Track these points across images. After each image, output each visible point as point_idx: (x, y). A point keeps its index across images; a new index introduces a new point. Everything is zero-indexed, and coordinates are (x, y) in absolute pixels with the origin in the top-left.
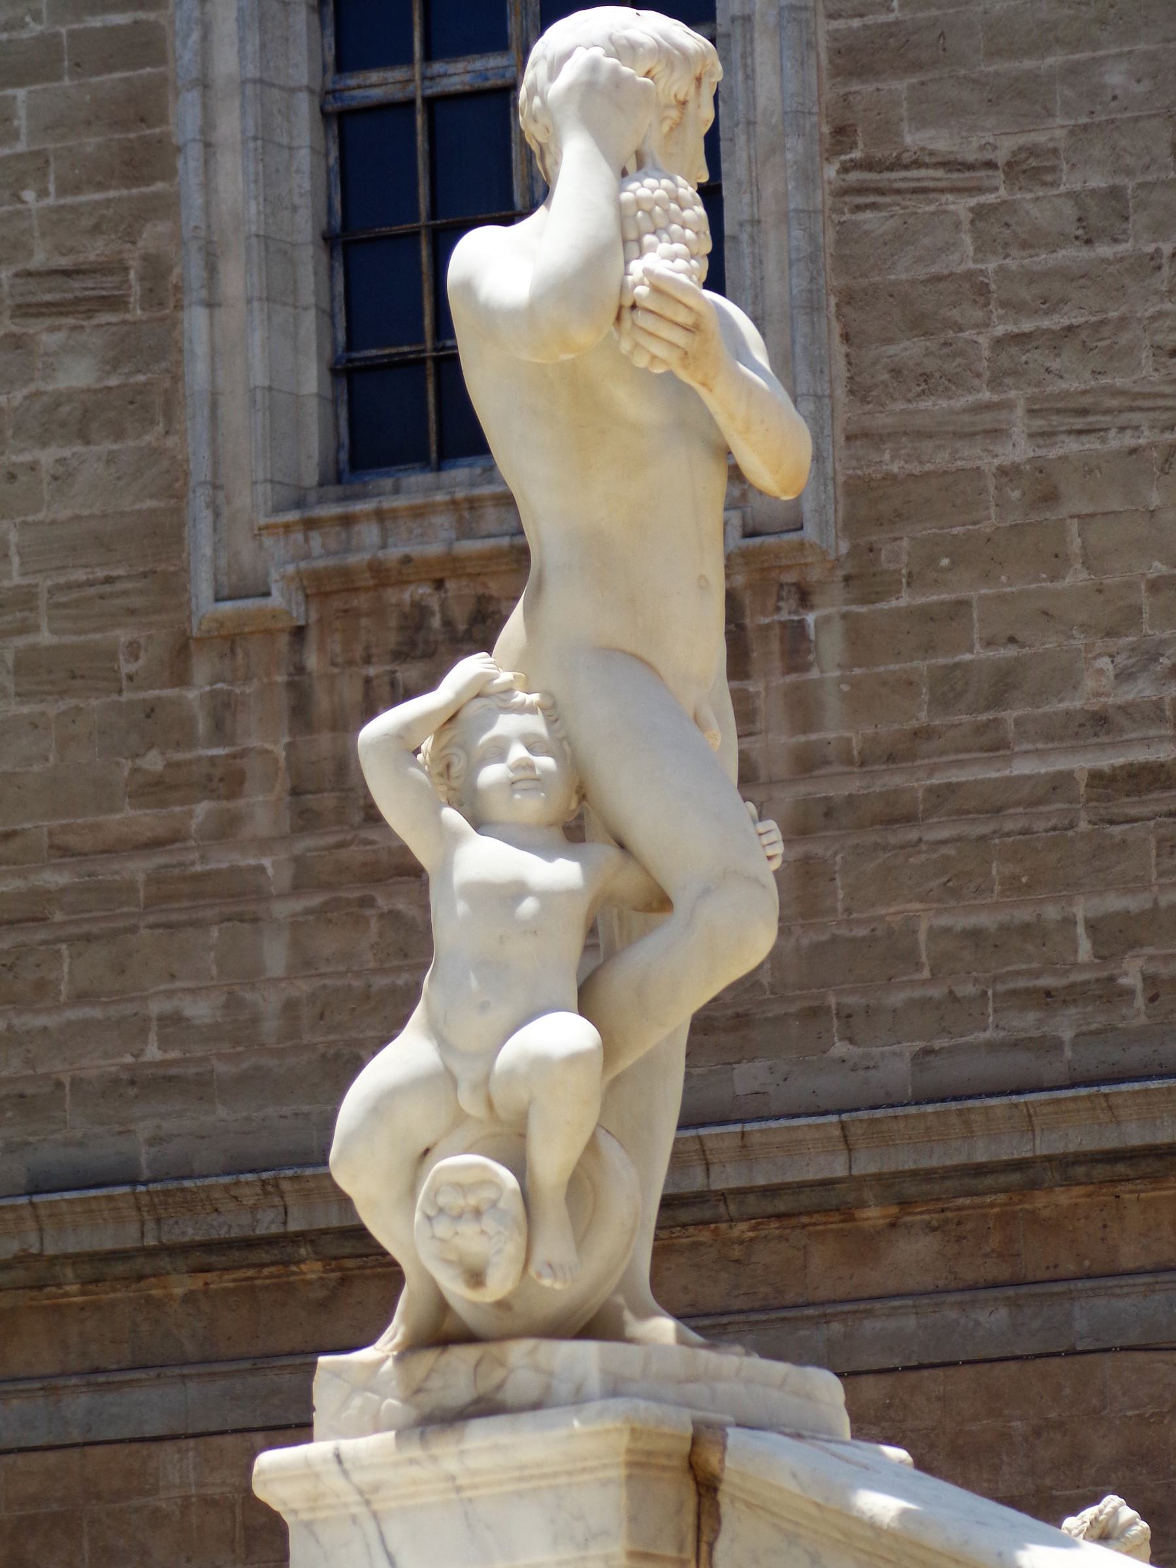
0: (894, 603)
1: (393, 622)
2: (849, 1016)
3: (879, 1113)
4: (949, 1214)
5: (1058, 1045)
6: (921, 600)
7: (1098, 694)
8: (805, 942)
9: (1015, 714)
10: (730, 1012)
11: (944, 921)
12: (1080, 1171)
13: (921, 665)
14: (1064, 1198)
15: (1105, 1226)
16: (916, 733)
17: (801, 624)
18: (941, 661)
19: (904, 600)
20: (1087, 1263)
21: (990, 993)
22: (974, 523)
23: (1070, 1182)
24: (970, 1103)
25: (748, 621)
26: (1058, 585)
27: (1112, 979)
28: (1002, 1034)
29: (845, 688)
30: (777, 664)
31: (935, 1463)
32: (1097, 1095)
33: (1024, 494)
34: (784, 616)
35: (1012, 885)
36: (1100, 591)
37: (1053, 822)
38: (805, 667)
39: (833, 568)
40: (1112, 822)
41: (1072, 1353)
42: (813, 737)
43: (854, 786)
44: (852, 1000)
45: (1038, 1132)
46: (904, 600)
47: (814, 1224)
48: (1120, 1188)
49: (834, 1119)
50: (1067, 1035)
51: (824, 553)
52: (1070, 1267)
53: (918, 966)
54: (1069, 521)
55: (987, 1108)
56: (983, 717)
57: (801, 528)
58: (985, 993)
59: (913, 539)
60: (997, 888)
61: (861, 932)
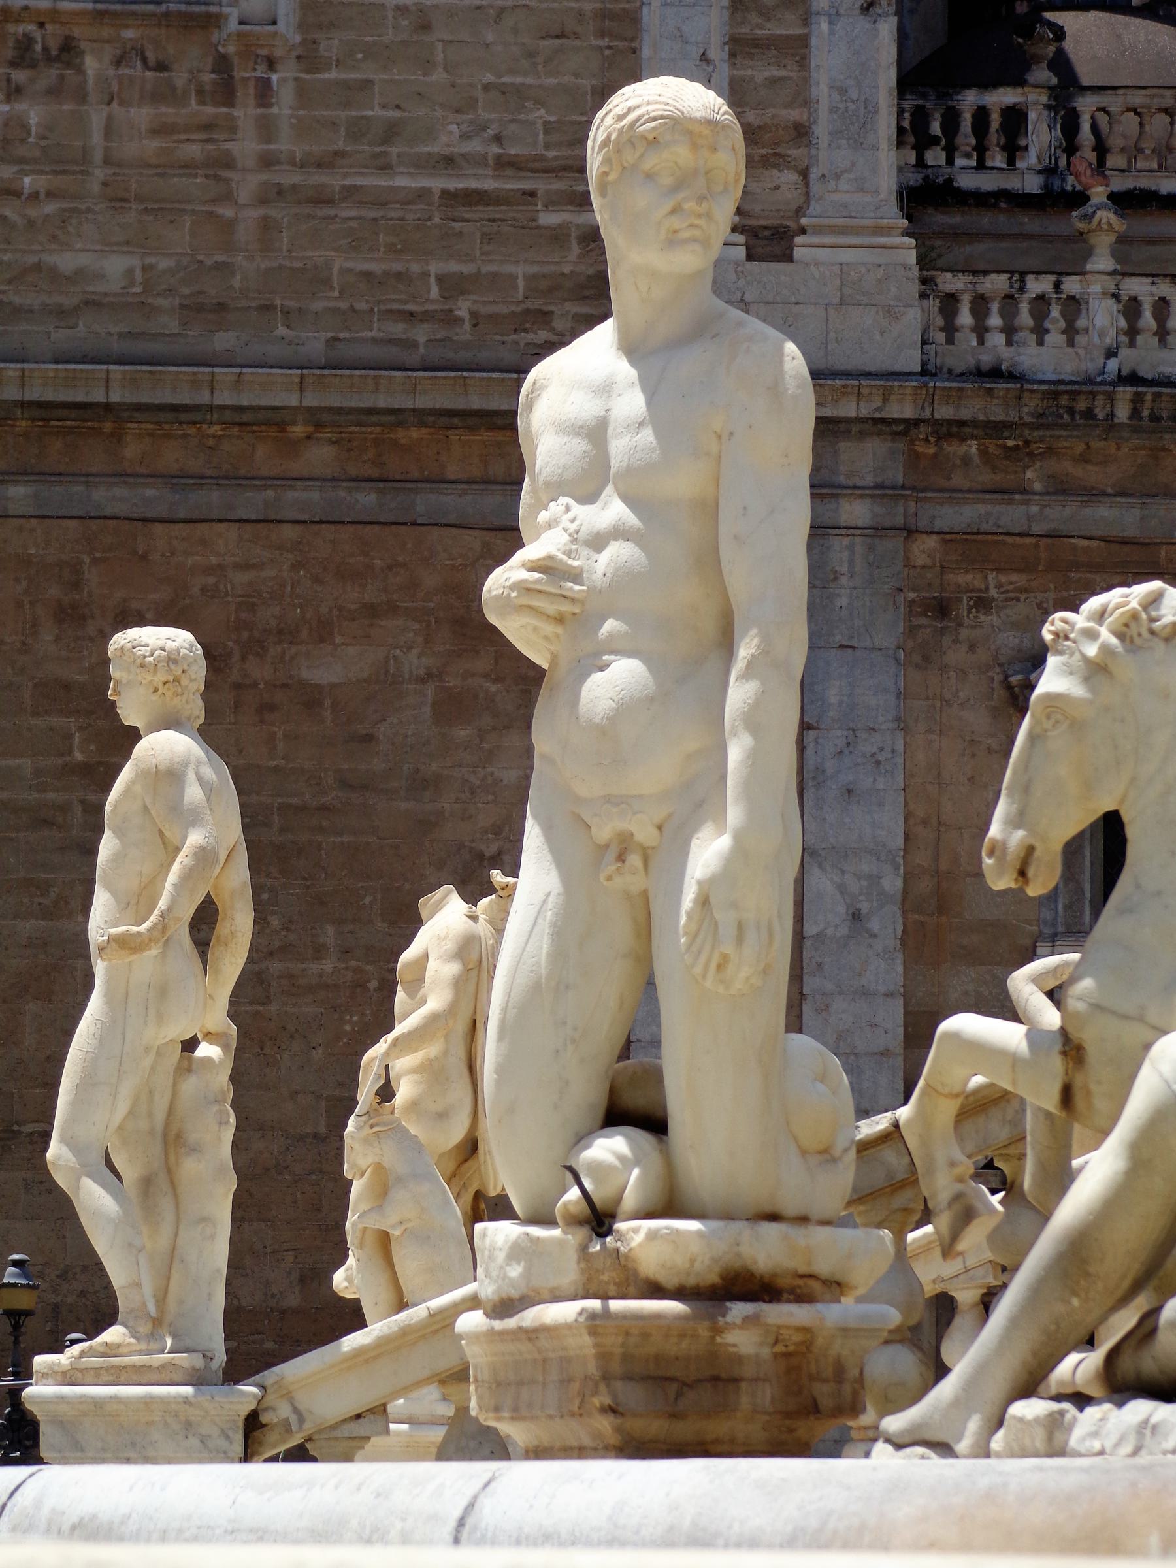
0: (327, 76)
1: (11, 44)
2: (288, 312)
3: (326, 372)
4: (343, 435)
5: (414, 345)
6: (343, 76)
7: (448, 145)
8: (263, 266)
9: (397, 150)
10: (214, 301)
11: (349, 264)
12: (431, 419)
13: (342, 114)
14: (415, 433)
15: (438, 453)
16: (336, 153)
17: (269, 80)
18: (354, 113)
19: (333, 74)
20: (426, 473)
21: (376, 310)
22: (379, 36)
23: (422, 424)
24: (383, 373)
25: (235, 73)
26: (427, 79)
27: (451, 311)
28: (382, 334)
29: (293, 121)
30: (252, 101)
31: (327, 579)
32: (459, 377)
33: (410, 23)
34: (258, 74)
35: (391, 248)
36: (453, 86)
37: (419, 215)
38: (269, 105)
39: (290, 50)
40: (454, 220)
41: (414, 524)
42: (272, 147)
43: (296, 178)
44: (291, 304)
45: (417, 395)
46: (333, 74)
47: (261, 432)
48: (449, 432)
49: (299, 371)
50: (422, 340)
51: (287, 40)
52: (416, 474)
53: (332, 288)
54: (437, 43)
55: (391, 377)
56: (378, 149)
57: (274, 23)
58: (372, 310)
59: (340, 40)
60: (382, 249)
61: (299, 265)
